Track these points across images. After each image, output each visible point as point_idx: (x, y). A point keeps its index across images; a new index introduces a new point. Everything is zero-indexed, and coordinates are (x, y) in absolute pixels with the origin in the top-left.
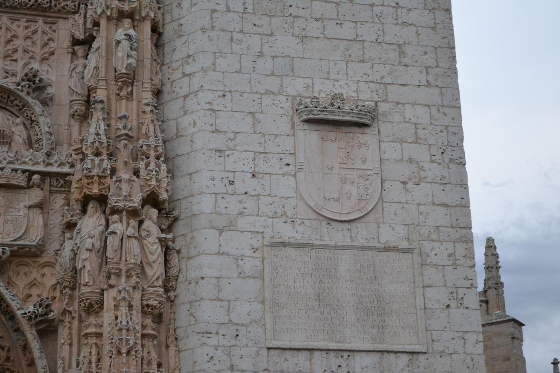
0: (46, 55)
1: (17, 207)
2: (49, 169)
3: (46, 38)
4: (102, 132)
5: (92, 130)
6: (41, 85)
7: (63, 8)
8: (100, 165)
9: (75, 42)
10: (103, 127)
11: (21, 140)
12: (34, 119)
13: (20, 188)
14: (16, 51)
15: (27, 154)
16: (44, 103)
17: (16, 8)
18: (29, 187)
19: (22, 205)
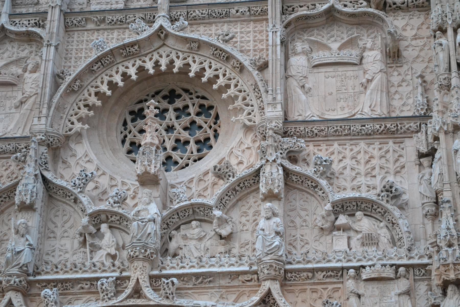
0: (399, 169)
1: (389, 295)
2: (411, 262)
3: (396, 155)
4: (451, 226)
5: (443, 226)
6: (397, 194)
7: (408, 129)
8: (453, 254)
9: (421, 156)
10: (452, 222)
11: (386, 240)
12: (394, 222)
13: (391, 279)
14: (374, 168)
15: (392, 251)
16: (401, 208)
17: (370, 134)
18: (397, 278)
19: (393, 293)
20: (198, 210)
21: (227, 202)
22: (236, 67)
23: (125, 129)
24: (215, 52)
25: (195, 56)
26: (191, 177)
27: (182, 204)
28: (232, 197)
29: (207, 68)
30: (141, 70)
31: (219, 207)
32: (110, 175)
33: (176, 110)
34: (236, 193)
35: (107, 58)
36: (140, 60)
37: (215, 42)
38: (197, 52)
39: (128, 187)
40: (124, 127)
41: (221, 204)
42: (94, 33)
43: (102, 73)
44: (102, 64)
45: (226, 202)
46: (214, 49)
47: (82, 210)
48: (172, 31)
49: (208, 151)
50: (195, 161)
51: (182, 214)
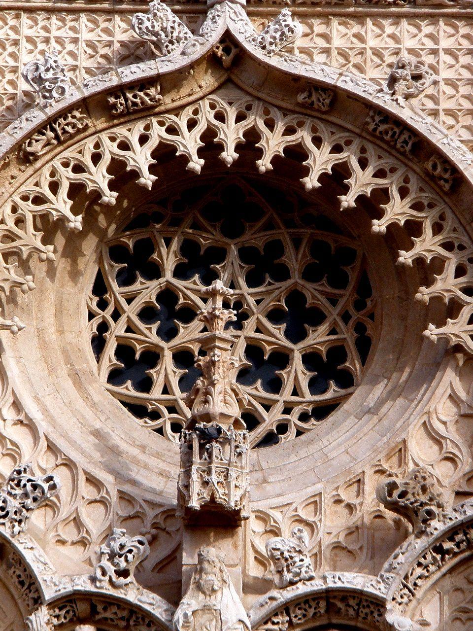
20: (340, 605)
21: (419, 582)
22: (441, 178)
23: (103, 305)
24: (382, 128)
25: (321, 126)
26: (311, 490)
27: (302, 589)
28: (432, 568)
29: (354, 163)
30: (166, 156)
31: (399, 600)
32: (85, 472)
33: (246, 255)
34: (443, 559)
35: (70, 119)
36: (161, 124)
37: (384, 101)
38: (325, 117)
39: (137, 508)
40: (96, 299)
41: (406, 591)
42: (18, 17)
43: (52, 159)
44: (57, 137)
45: (415, 584)
46: (377, 119)
47: (22, 583)
48: (259, 54)
49: (343, 392)
50: (304, 417)
51: (299, 612)
